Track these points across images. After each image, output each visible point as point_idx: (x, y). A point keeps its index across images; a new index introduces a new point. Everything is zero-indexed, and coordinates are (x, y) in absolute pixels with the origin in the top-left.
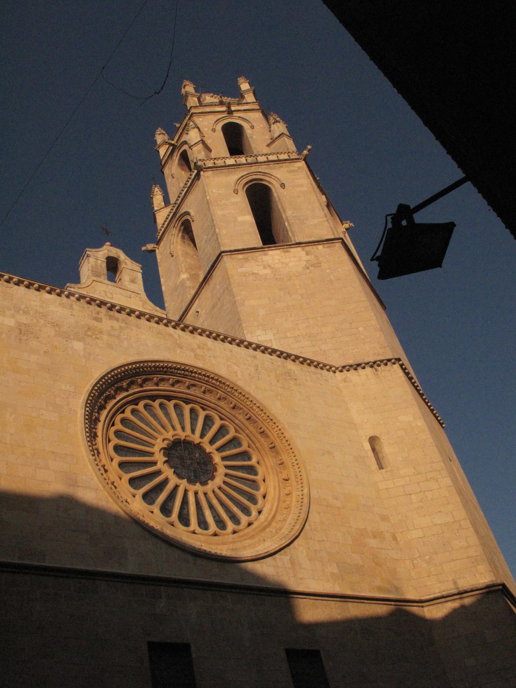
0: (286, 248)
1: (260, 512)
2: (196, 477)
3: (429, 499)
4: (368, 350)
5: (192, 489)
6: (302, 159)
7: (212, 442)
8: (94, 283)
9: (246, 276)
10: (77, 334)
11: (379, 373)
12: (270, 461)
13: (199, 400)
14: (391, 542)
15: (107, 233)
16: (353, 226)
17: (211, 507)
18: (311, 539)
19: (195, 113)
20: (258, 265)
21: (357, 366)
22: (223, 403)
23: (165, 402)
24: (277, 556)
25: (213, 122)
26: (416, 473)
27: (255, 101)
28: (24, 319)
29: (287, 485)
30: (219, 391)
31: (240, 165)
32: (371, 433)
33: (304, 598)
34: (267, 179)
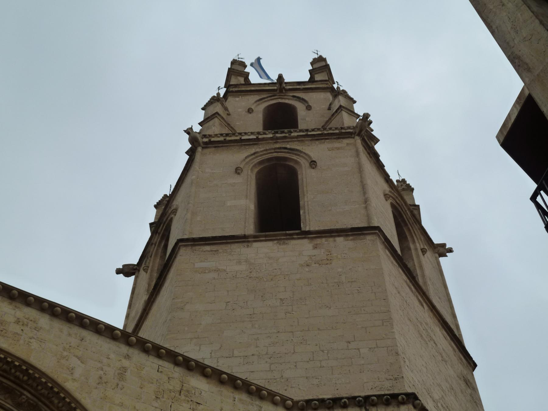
0: (284, 239)
4: (365, 381)
6: (356, 134)
25: (253, 102)
30: (25, 393)
34: (294, 157)
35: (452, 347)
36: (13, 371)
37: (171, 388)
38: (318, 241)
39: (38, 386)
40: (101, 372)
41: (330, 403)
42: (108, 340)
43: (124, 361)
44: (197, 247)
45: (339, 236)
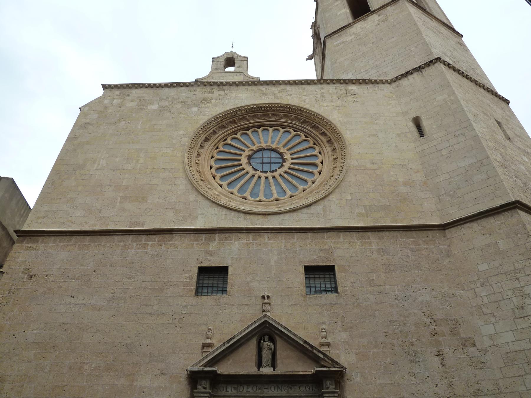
0: (365, 18)
1: (313, 183)
3: (456, 150)
7: (272, 142)
8: (213, 74)
11: (423, 73)
13: (279, 123)
14: (421, 187)
18: (345, 192)
21: (408, 74)
22: (296, 121)
24: (312, 207)
26: (447, 134)
28: (163, 104)
29: (336, 162)
30: (292, 115)
32: (414, 115)
35: (450, 32)
36: (285, 109)
37: (342, 93)
38: (380, 12)
39: (295, 111)
40: (315, 98)
41: (405, 75)
42: (313, 85)
43: (322, 90)
44: (333, 37)
45: (388, 6)
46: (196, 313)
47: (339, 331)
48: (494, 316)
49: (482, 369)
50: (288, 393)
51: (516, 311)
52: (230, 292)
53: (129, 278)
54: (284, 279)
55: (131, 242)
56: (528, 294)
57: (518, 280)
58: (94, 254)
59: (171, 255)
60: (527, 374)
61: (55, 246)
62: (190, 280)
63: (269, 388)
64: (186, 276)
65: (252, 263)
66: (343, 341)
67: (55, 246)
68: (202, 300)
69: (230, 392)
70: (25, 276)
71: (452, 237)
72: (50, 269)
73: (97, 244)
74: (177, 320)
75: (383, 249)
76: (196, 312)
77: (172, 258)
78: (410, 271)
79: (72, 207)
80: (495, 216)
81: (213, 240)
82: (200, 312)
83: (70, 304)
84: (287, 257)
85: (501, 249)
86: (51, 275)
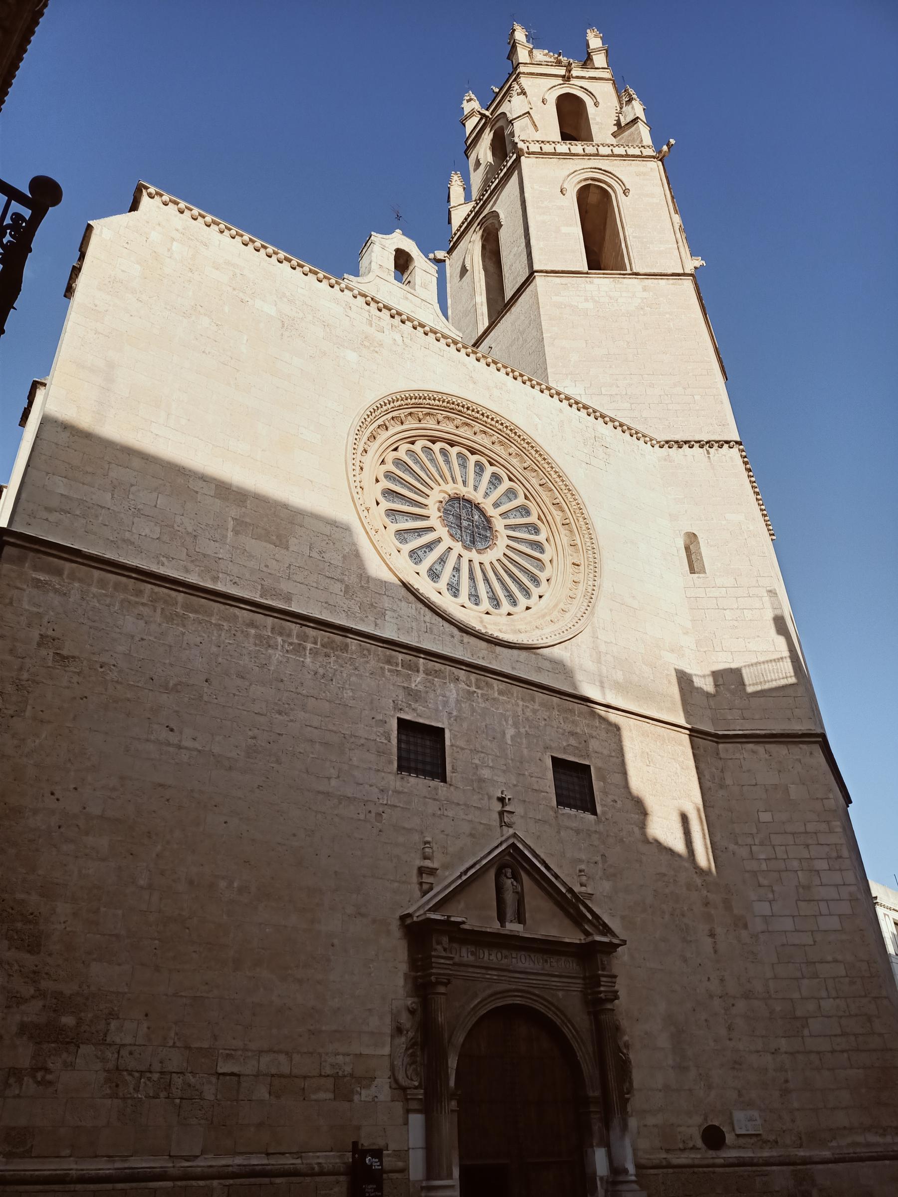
2: (473, 542)
5: (467, 555)
9: (562, 308)
10: (352, 342)
12: (563, 538)
15: (399, 217)
16: (705, 265)
17: (486, 579)
19: (524, 73)
20: (578, 296)
23: (447, 447)
25: (546, 89)
27: (606, 67)
31: (574, 155)
33: (581, 704)
46: (402, 808)
47: (601, 878)
48: (773, 891)
49: (753, 962)
50: (543, 969)
51: (801, 890)
52: (451, 779)
53: (280, 713)
54: (526, 773)
55: (272, 633)
56: (818, 871)
57: (808, 848)
58: (199, 640)
59: (348, 682)
60: (803, 978)
61: (106, 595)
62: (385, 742)
63: (519, 955)
64: (379, 732)
65: (479, 732)
66: (605, 894)
67: (106, 595)
68: (409, 785)
69: (465, 959)
70: (47, 654)
71: (728, 757)
72: (107, 651)
73: (200, 617)
74: (373, 814)
75: (648, 754)
76: (401, 805)
77: (351, 687)
78: (680, 799)
79: (126, 507)
80: (790, 746)
81: (416, 669)
82: (409, 807)
83: (169, 744)
84: (527, 733)
85: (791, 798)
86: (112, 667)
